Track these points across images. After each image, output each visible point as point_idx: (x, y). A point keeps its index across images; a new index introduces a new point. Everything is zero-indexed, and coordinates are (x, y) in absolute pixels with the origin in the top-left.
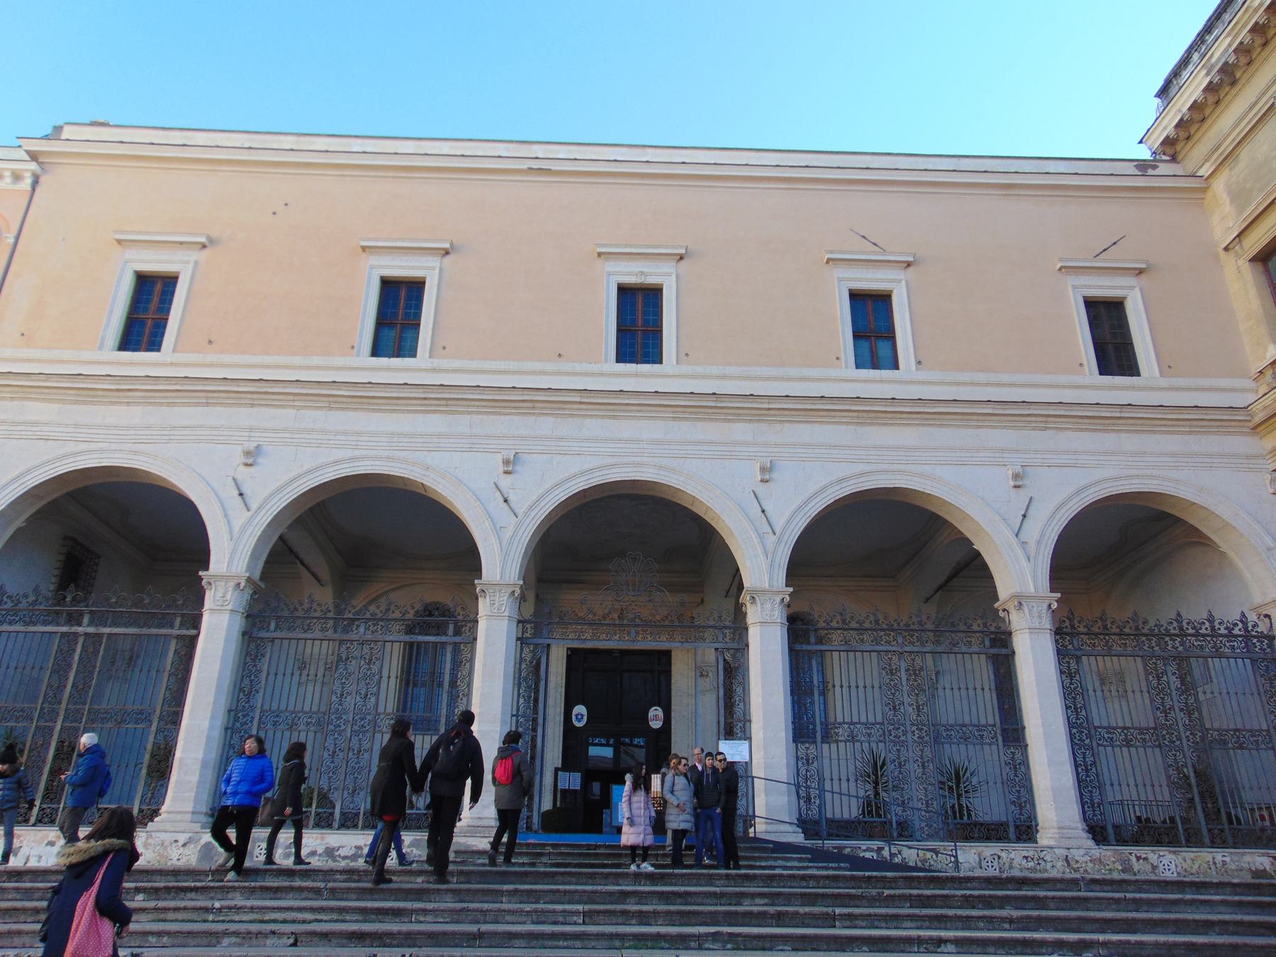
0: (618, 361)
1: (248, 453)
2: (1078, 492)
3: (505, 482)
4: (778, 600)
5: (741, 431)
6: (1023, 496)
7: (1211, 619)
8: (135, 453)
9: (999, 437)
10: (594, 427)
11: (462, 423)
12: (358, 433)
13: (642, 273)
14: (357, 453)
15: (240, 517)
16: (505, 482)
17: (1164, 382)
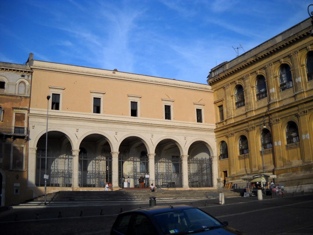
0: (131, 116)
1: (77, 130)
2: (192, 140)
3: (116, 136)
4: (154, 155)
5: (149, 129)
6: (186, 141)
7: (206, 158)
8: (59, 129)
9: (184, 131)
10: (128, 127)
11: (109, 125)
12: (93, 127)
13: (135, 100)
14: (93, 130)
15: (77, 140)
16: (116, 136)
17: (205, 124)
